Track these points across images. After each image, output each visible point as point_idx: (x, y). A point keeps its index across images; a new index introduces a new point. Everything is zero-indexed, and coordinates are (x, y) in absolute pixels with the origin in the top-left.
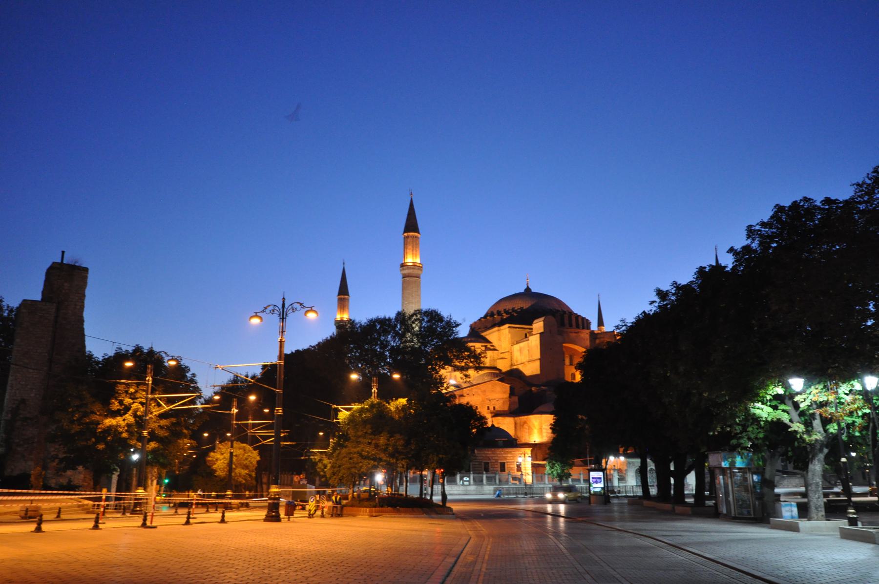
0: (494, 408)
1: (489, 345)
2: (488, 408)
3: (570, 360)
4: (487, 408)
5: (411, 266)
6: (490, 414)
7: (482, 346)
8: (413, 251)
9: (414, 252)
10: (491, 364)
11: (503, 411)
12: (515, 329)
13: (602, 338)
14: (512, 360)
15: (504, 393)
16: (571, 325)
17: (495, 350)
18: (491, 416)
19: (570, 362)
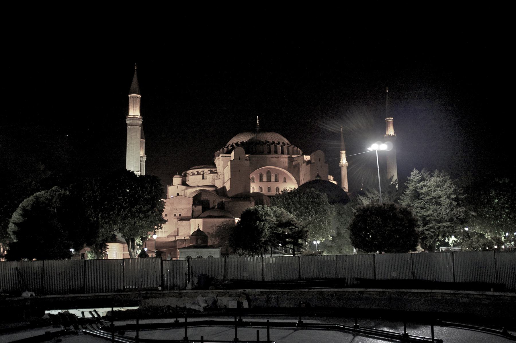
0: (180, 215)
1: (214, 169)
2: (175, 215)
3: (275, 178)
5: (131, 117)
6: (177, 219)
7: (208, 171)
8: (133, 107)
9: (135, 108)
10: (212, 183)
12: (226, 158)
13: (297, 161)
14: (224, 180)
15: (189, 204)
16: (276, 152)
17: (217, 173)
19: (275, 180)
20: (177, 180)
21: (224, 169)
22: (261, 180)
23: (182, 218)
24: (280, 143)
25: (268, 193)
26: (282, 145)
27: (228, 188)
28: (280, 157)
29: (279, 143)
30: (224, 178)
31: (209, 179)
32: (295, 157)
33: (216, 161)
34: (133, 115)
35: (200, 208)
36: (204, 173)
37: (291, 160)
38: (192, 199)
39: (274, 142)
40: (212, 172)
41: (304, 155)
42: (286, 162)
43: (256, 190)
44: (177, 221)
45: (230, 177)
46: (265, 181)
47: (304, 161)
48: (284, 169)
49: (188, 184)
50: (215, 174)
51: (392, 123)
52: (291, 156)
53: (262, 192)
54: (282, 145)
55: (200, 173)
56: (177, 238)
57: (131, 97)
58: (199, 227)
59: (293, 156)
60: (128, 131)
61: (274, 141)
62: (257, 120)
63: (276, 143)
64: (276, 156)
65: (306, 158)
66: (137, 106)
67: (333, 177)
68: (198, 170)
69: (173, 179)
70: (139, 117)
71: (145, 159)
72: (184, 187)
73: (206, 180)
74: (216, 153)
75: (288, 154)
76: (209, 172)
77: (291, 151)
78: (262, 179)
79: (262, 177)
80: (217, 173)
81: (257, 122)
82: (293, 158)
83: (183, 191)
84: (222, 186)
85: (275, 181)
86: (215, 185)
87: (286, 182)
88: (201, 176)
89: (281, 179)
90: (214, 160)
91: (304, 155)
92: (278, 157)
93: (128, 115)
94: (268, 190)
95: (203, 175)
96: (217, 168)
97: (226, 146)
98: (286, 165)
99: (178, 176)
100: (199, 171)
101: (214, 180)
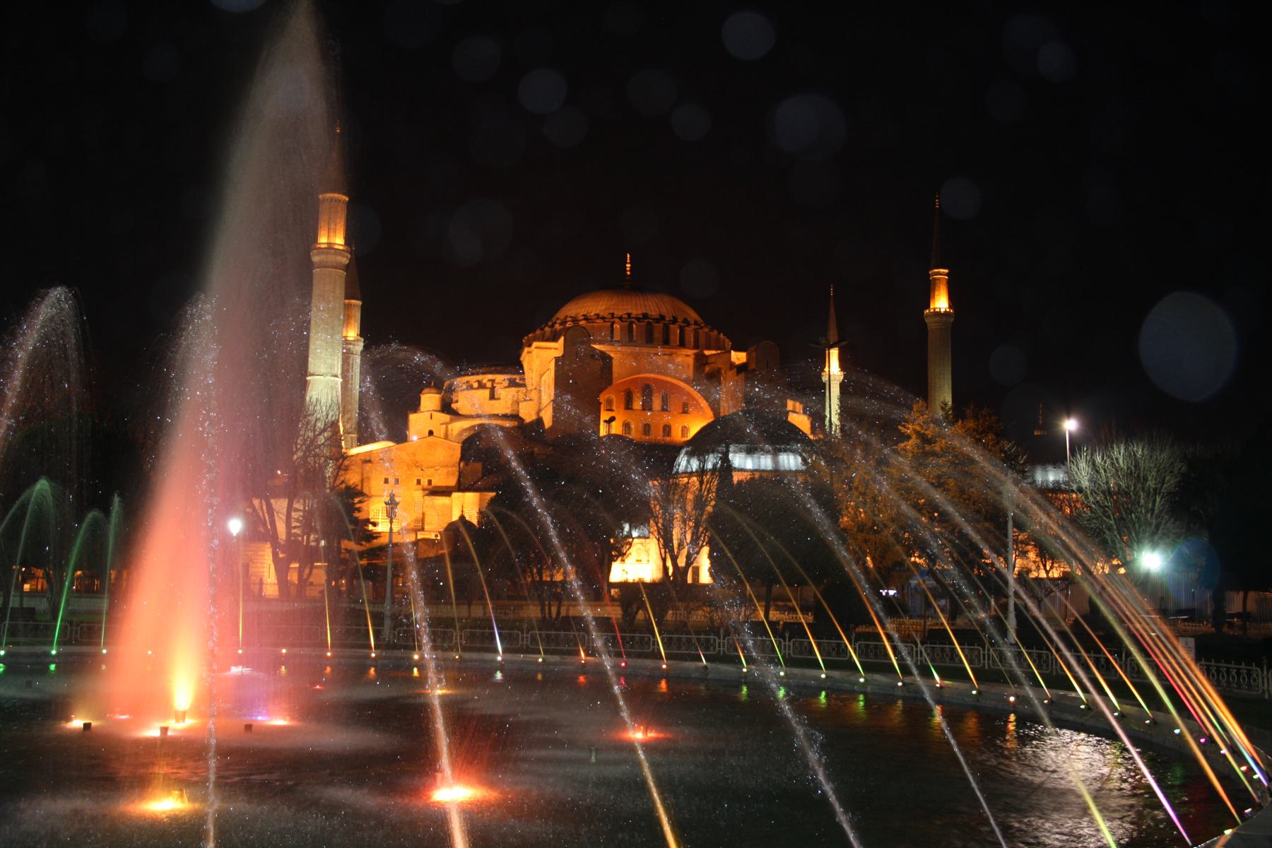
0: (430, 482)
1: (517, 378)
4: (416, 482)
5: (323, 248)
8: (329, 224)
9: (332, 226)
10: (514, 410)
11: (447, 487)
14: (540, 403)
17: (524, 385)
18: (422, 495)
20: (430, 400)
21: (541, 378)
22: (628, 406)
23: (434, 489)
24: (679, 320)
25: (643, 436)
26: (682, 324)
27: (548, 422)
28: (676, 353)
29: (674, 321)
30: (540, 398)
31: (506, 399)
32: (711, 355)
33: (524, 359)
34: (328, 243)
35: (479, 466)
36: (495, 385)
37: (700, 361)
38: (460, 445)
39: (662, 318)
40: (512, 384)
41: (733, 352)
42: (689, 366)
43: (616, 428)
44: (423, 496)
45: (552, 398)
46: (637, 410)
47: (732, 365)
48: (685, 381)
49: (455, 408)
50: (520, 389)
51: (945, 282)
52: (702, 351)
53: (629, 433)
54: (682, 324)
55: (485, 384)
56: (420, 537)
57: (324, 200)
58: (462, 511)
59: (707, 353)
60: (315, 282)
61: (662, 313)
62: (627, 263)
63: (667, 319)
64: (666, 350)
65: (738, 359)
66: (338, 221)
67: (801, 406)
68: (480, 377)
69: (420, 398)
70: (341, 248)
71: (359, 347)
72: (446, 417)
73: (498, 401)
74: (526, 338)
75: (696, 347)
76: (506, 383)
77: (702, 340)
78: (632, 405)
79: (632, 398)
80: (524, 385)
81: (626, 267)
82: (707, 357)
83: (444, 426)
84: (534, 417)
85: (663, 410)
86: (518, 415)
88: (486, 393)
89: (675, 405)
90: (520, 355)
91: (732, 351)
92: (670, 355)
93: (315, 240)
94: (645, 431)
95: (492, 390)
96: (527, 376)
97: (550, 324)
98: (690, 373)
99: (434, 391)
100: (482, 381)
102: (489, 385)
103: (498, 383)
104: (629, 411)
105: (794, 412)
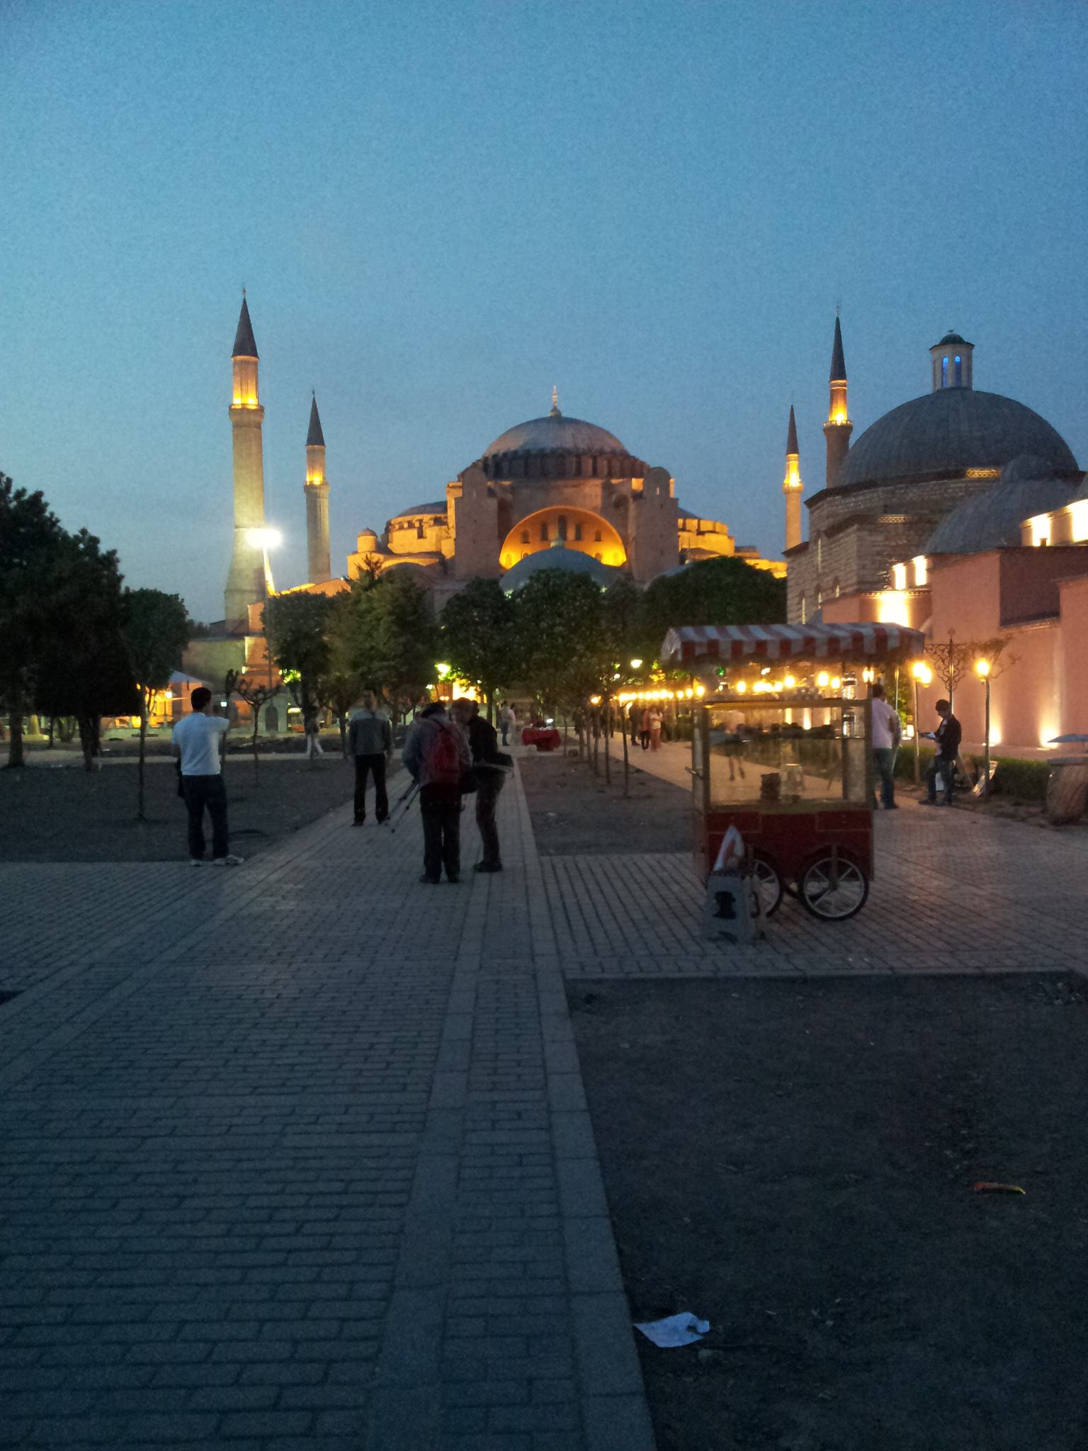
1: (442, 516)
8: (241, 385)
9: (244, 388)
19: (576, 535)
34: (243, 404)
37: (608, 489)
42: (596, 496)
48: (594, 509)
52: (609, 481)
59: (614, 481)
76: (432, 522)
87: (602, 539)
88: (415, 532)
89: (589, 534)
98: (598, 502)
101: (439, 539)
102: (417, 525)
103: (425, 523)
104: (545, 542)
105: (713, 532)
